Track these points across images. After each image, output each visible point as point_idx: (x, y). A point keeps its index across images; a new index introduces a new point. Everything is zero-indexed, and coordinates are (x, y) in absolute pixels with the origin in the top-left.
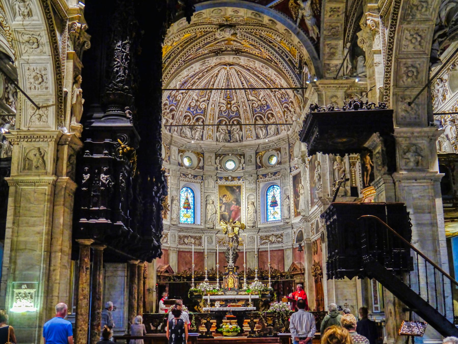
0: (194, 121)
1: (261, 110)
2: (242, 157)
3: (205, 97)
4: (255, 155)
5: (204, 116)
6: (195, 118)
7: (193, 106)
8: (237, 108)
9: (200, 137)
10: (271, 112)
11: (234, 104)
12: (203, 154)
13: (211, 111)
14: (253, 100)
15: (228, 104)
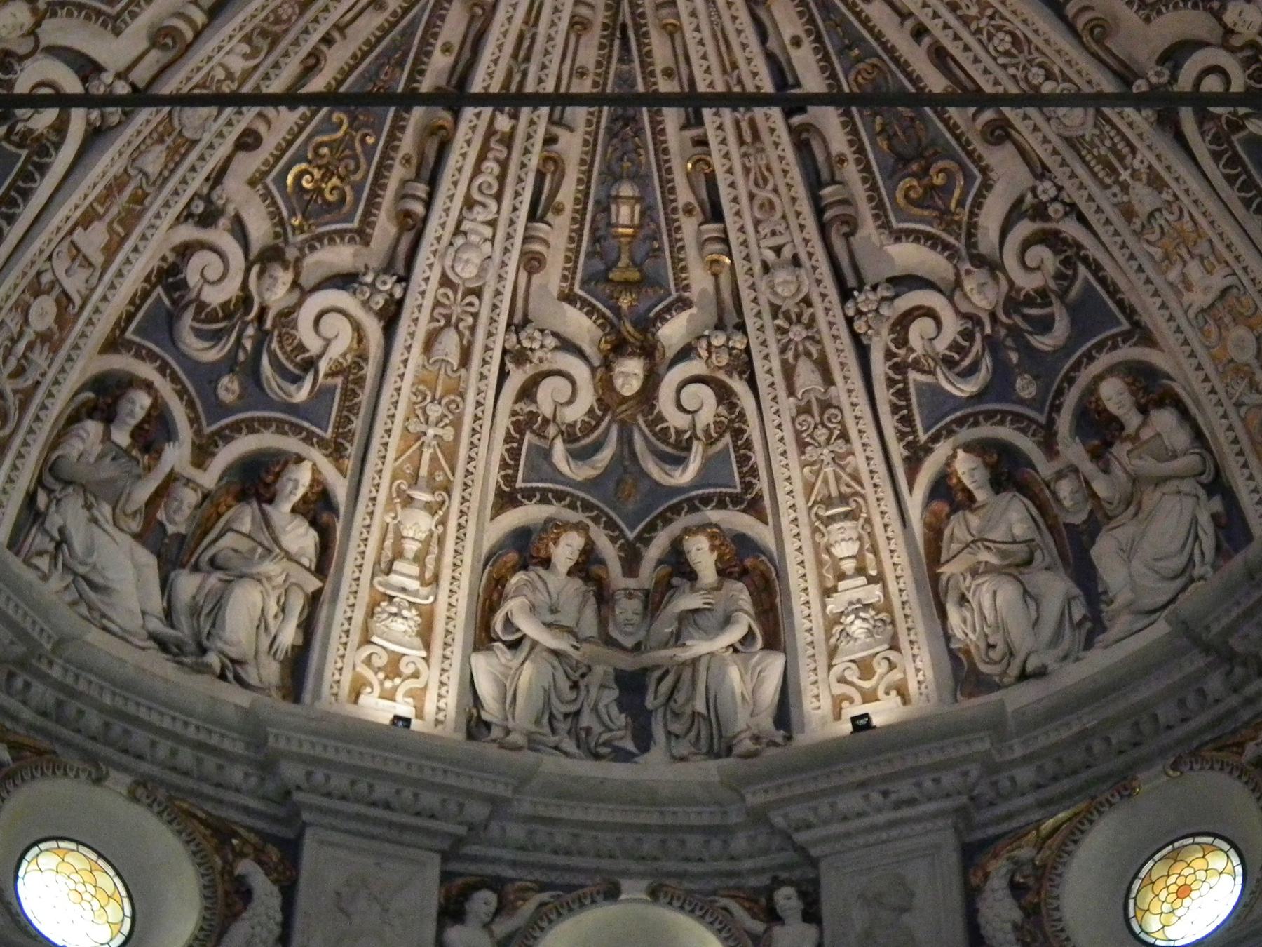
0: (209, 478)
1: (1000, 385)
2: (787, 899)
3: (362, 236)
4: (951, 858)
5: (336, 452)
6: (227, 455)
7: (215, 297)
8: (724, 395)
9: (271, 671)
10: (1128, 352)
11: (686, 353)
12: (291, 850)
13: (417, 411)
14: (906, 282)
15: (619, 348)
